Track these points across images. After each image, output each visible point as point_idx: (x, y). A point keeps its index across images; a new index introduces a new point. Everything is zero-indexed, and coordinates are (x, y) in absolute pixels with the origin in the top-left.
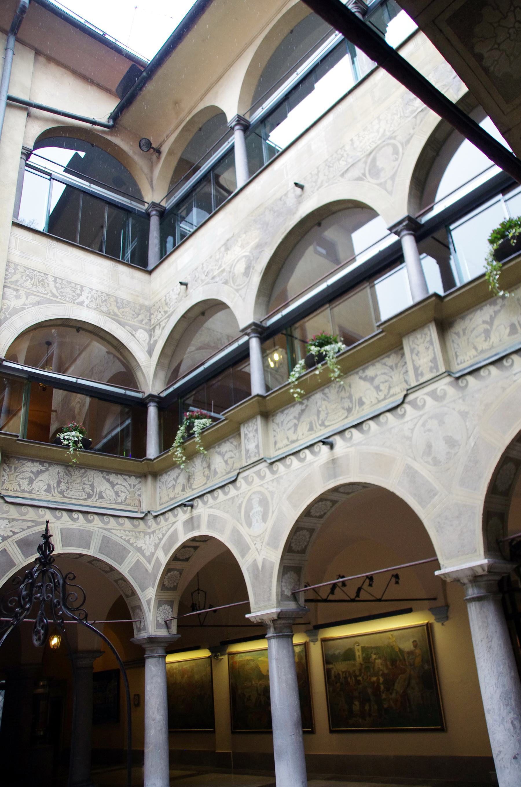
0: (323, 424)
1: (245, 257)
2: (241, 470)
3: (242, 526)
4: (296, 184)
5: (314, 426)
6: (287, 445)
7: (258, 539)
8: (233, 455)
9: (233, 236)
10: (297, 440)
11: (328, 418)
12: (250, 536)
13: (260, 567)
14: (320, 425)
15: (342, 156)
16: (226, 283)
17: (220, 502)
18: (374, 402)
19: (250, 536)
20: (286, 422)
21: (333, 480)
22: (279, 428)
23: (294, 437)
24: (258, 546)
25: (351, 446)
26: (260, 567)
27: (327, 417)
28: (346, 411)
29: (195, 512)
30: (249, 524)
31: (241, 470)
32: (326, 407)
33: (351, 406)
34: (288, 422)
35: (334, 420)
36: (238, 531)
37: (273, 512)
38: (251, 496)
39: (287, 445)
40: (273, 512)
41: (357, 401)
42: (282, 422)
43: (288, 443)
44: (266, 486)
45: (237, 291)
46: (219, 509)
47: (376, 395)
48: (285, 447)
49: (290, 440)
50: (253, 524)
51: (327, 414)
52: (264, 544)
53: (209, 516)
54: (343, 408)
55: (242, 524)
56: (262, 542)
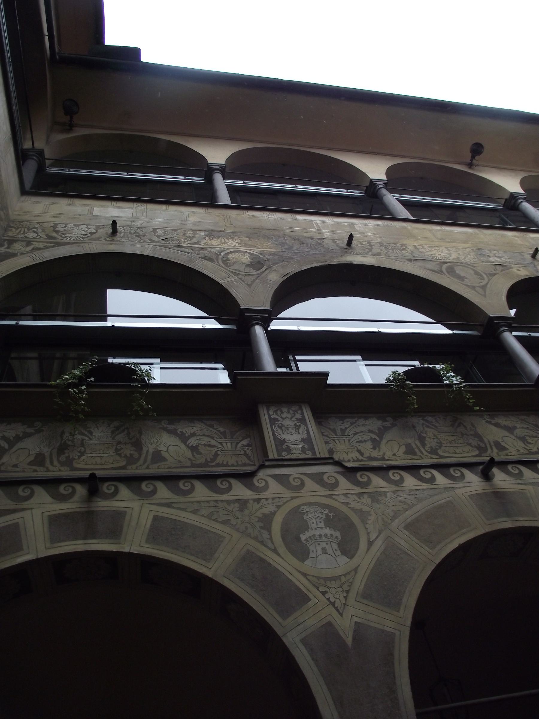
0: (433, 452)
1: (251, 254)
2: (267, 463)
3: (279, 555)
4: (351, 237)
5: (416, 450)
6: (358, 460)
7: (333, 584)
8: (213, 442)
9: (223, 231)
10: (383, 459)
11: (443, 448)
12: (305, 575)
13: (349, 641)
14: (428, 452)
15: (404, 249)
16: (210, 260)
17: (199, 502)
18: (521, 451)
19: (305, 575)
20: (352, 432)
21: (505, 519)
22: (336, 435)
23: (375, 454)
24: (336, 595)
25: (525, 484)
26: (349, 641)
27: (440, 447)
28: (475, 449)
29: (102, 505)
30: (302, 553)
31: (267, 463)
32: (435, 435)
33: (482, 445)
34: (356, 433)
35: (456, 453)
36: (262, 560)
37: (370, 544)
38: (299, 507)
39: (358, 460)
40: (370, 544)
41: (492, 444)
42: (343, 431)
43: (361, 458)
44: (342, 499)
45: (235, 274)
46: (195, 512)
47: (524, 446)
48: (354, 461)
49: (365, 455)
50: (312, 555)
51: (440, 445)
52: (352, 595)
53: (156, 518)
54: (470, 445)
55: (275, 551)
56: (348, 592)
